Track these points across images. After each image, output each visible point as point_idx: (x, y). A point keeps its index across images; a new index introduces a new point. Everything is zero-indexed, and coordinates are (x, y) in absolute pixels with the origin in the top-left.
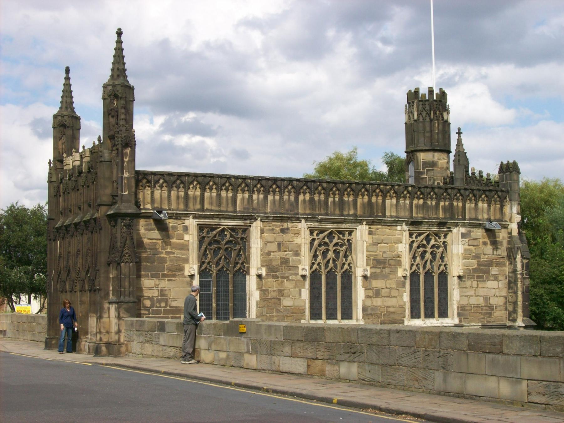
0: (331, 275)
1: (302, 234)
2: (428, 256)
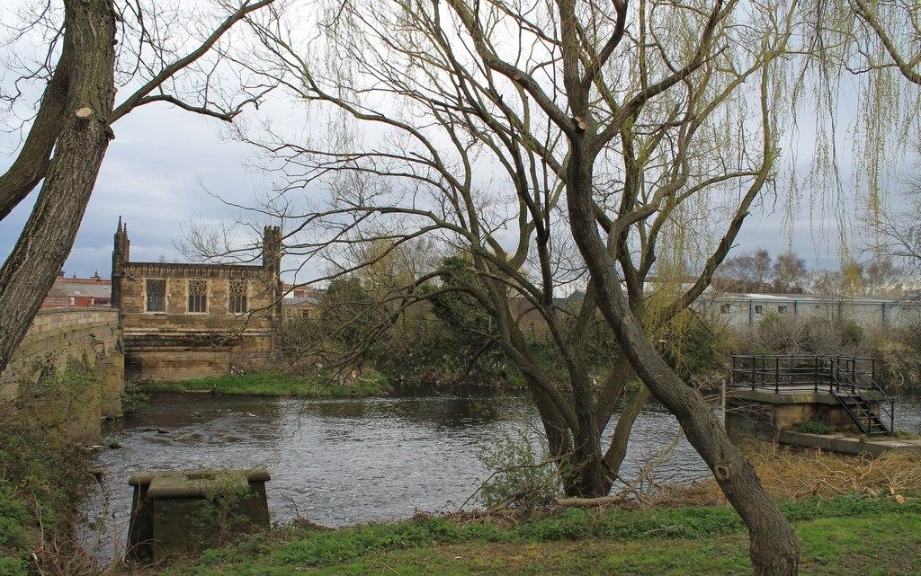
0: (197, 297)
1: (186, 282)
2: (238, 291)
